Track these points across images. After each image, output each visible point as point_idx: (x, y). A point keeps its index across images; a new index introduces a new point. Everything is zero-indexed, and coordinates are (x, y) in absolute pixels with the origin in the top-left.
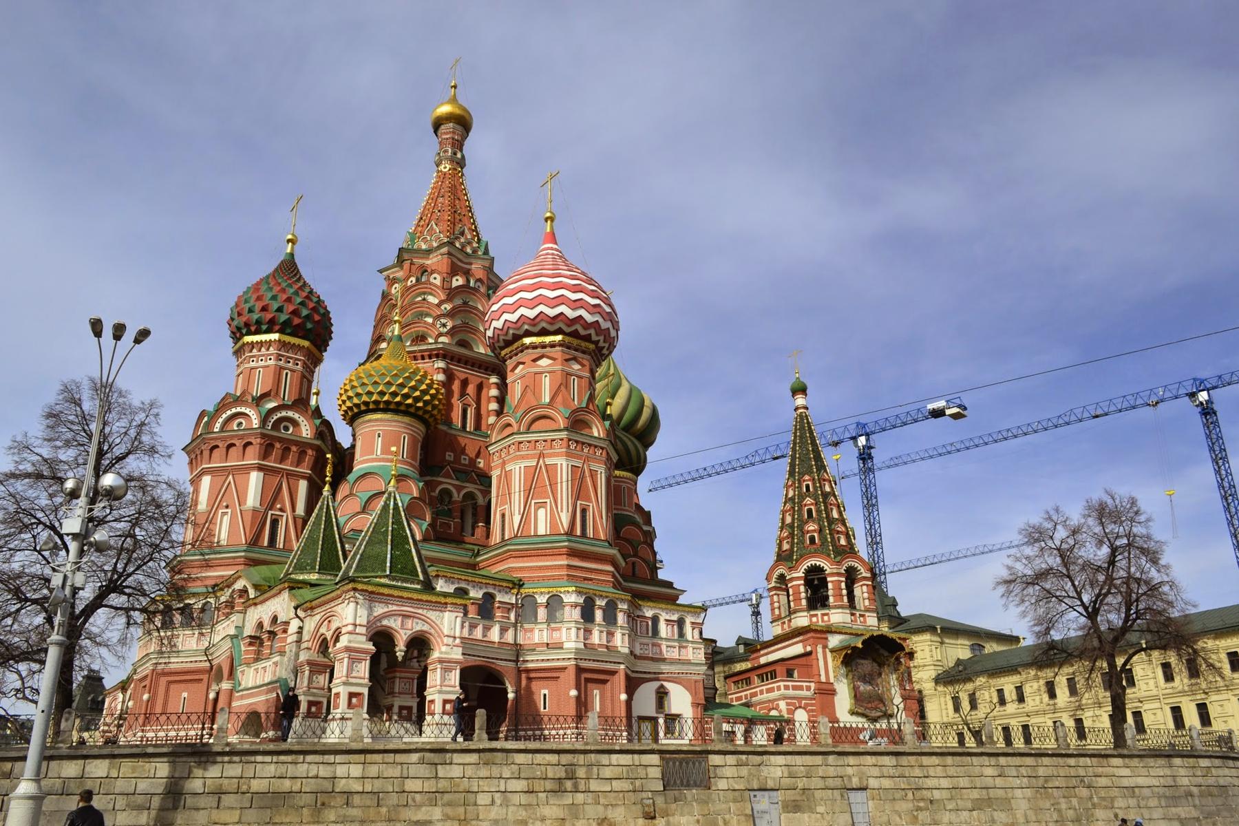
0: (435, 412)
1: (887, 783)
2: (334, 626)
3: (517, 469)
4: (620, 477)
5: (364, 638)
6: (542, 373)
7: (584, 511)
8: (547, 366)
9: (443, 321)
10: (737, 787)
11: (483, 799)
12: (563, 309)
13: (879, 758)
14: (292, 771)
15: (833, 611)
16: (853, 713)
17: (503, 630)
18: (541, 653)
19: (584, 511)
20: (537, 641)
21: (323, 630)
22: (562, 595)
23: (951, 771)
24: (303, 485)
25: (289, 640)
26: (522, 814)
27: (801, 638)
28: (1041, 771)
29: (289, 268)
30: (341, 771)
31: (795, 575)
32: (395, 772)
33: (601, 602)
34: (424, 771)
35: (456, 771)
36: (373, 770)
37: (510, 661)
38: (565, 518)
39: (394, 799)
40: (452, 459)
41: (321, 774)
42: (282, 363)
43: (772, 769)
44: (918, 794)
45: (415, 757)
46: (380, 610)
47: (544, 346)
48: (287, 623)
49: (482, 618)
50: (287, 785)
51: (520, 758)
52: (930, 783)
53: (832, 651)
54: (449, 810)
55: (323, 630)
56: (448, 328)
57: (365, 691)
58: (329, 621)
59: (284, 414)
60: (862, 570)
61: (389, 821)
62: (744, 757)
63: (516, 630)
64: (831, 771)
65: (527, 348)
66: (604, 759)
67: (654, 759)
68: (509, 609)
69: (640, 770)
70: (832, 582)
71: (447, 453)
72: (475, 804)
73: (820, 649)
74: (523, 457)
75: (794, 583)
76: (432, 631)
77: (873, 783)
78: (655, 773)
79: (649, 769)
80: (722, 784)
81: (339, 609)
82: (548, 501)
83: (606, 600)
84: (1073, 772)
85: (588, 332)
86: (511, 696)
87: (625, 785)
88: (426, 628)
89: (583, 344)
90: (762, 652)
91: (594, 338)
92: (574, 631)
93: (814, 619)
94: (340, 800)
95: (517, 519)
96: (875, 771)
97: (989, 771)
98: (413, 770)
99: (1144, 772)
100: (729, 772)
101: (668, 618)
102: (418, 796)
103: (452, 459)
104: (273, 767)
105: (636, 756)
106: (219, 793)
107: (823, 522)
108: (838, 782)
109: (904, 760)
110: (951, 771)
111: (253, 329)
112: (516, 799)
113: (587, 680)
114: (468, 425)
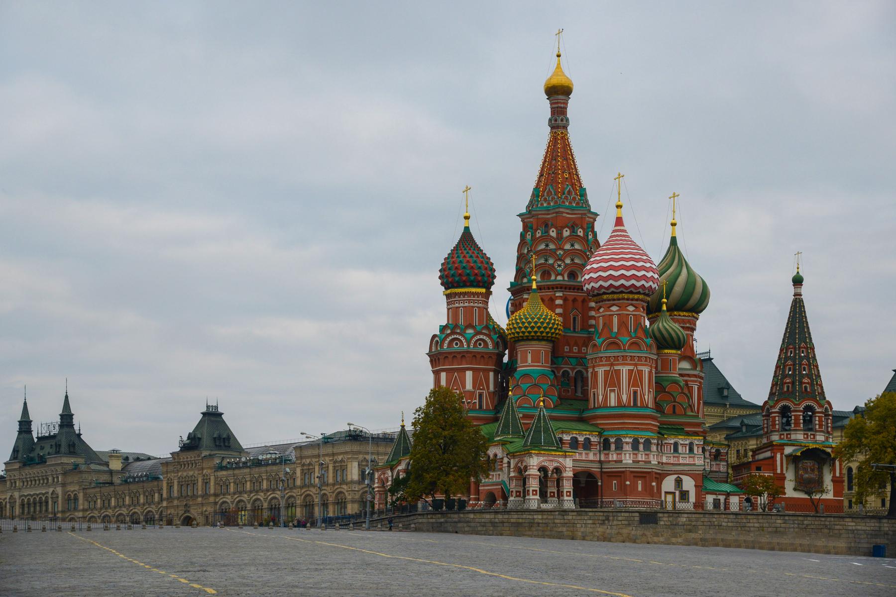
0: (557, 331)
1: (730, 524)
2: (524, 464)
3: (601, 371)
4: (667, 353)
5: (536, 471)
6: (614, 315)
7: (635, 392)
8: (615, 311)
9: (559, 263)
10: (667, 524)
11: (578, 526)
12: (622, 282)
13: (728, 515)
14: (522, 517)
15: (792, 433)
16: (795, 489)
17: (595, 454)
18: (613, 465)
19: (635, 392)
20: (610, 459)
21: (519, 465)
22: (622, 438)
23: (761, 521)
24: (491, 374)
25: (504, 465)
26: (591, 530)
27: (770, 448)
28: (805, 522)
29: (467, 237)
30: (535, 517)
31: (773, 410)
32: (552, 517)
33: (642, 441)
34: (560, 517)
35: (570, 517)
36: (545, 517)
37: (598, 468)
38: (624, 398)
39: (552, 525)
40: (568, 350)
41: (530, 518)
42: (472, 304)
43: (682, 518)
44: (743, 529)
45: (557, 513)
46: (542, 459)
47: (614, 300)
48: (502, 458)
49: (584, 450)
50: (521, 521)
51: (590, 514)
52: (749, 525)
53: (785, 456)
54: (568, 528)
55: (519, 465)
56: (562, 267)
57: (538, 489)
58: (522, 462)
59: (478, 337)
60: (816, 408)
61: (551, 531)
62: (671, 514)
63: (600, 454)
64: (706, 520)
65: (605, 300)
66: (619, 514)
67: (637, 514)
68: (597, 444)
69: (632, 518)
70: (794, 415)
71: (566, 347)
72: (576, 527)
73: (778, 456)
74: (603, 365)
75: (773, 415)
76: (561, 466)
77: (723, 524)
78: (637, 519)
79: (635, 518)
80: (662, 523)
81: (525, 459)
82: (616, 389)
83: (644, 440)
84: (822, 523)
85: (638, 290)
86: (600, 484)
87: (626, 522)
88: (559, 464)
89: (636, 296)
90: (757, 452)
91: (642, 292)
92: (628, 455)
93: (782, 437)
94: (536, 525)
95: (601, 398)
96: (726, 520)
97: (779, 521)
98: (557, 517)
99: (864, 524)
100: (665, 519)
101: (682, 442)
102: (559, 525)
103: (568, 350)
104: (516, 516)
105: (630, 514)
106: (503, 523)
107: (796, 377)
108: (709, 523)
109: (739, 517)
110: (761, 521)
111: (455, 285)
112: (589, 526)
113: (634, 476)
114: (577, 327)
